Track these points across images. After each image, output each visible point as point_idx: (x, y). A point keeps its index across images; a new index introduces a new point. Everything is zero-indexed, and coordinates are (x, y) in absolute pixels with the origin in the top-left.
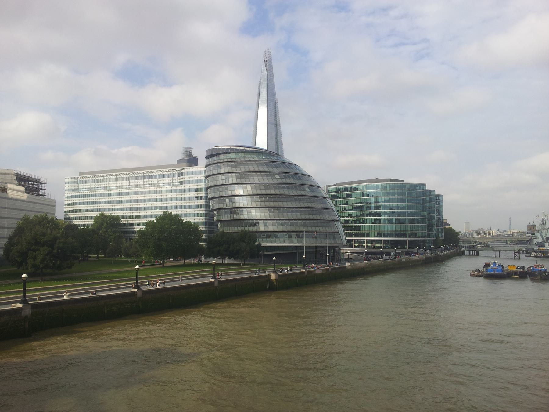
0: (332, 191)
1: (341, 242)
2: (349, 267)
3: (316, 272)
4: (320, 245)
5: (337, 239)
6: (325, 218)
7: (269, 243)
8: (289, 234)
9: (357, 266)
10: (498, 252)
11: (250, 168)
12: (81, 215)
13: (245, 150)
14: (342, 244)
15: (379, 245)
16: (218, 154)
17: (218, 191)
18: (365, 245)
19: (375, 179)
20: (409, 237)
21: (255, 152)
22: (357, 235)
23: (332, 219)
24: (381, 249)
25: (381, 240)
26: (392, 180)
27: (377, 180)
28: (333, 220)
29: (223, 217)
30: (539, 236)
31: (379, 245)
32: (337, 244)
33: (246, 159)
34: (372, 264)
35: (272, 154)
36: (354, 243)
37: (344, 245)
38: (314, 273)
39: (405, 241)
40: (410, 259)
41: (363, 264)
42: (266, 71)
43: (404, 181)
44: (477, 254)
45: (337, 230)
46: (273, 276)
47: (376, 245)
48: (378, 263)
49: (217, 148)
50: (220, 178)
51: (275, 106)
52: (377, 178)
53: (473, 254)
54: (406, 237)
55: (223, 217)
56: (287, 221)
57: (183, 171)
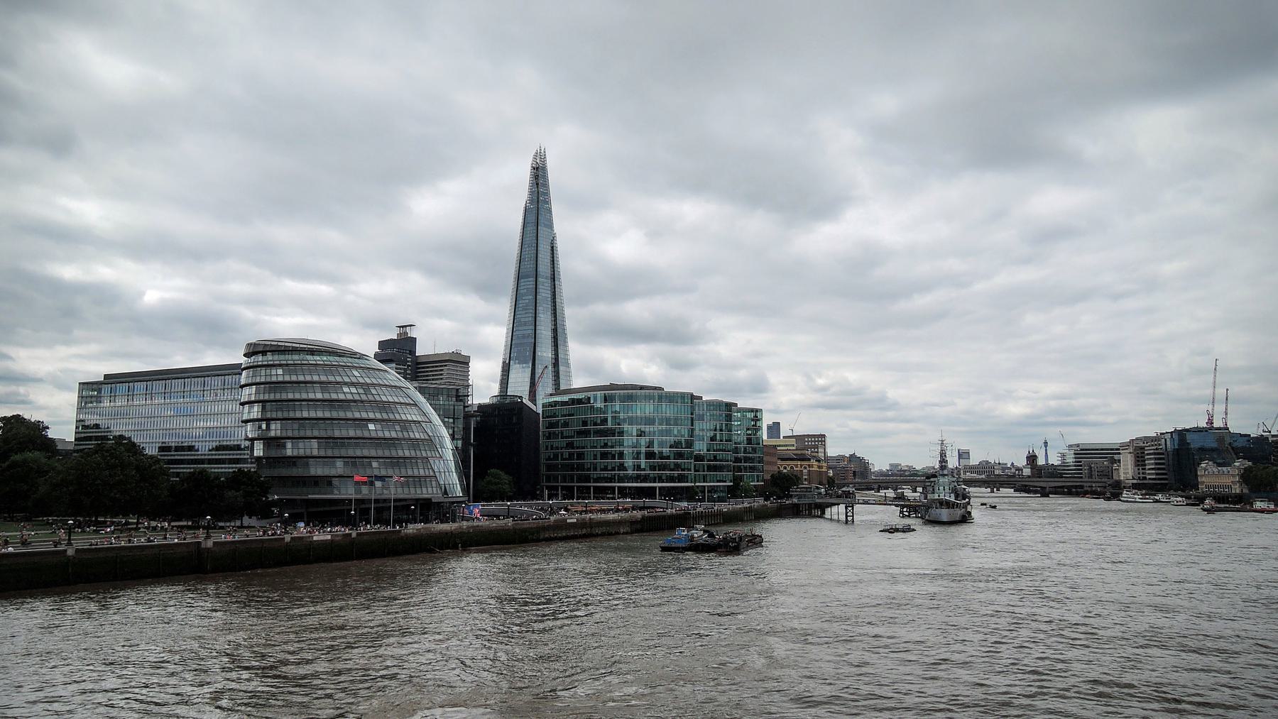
4: (379, 497)
7: (310, 494)
15: (611, 496)
31: (611, 496)
34: (478, 526)
38: (311, 540)
39: (654, 488)
42: (536, 186)
45: (432, 474)
51: (552, 247)
54: (655, 482)
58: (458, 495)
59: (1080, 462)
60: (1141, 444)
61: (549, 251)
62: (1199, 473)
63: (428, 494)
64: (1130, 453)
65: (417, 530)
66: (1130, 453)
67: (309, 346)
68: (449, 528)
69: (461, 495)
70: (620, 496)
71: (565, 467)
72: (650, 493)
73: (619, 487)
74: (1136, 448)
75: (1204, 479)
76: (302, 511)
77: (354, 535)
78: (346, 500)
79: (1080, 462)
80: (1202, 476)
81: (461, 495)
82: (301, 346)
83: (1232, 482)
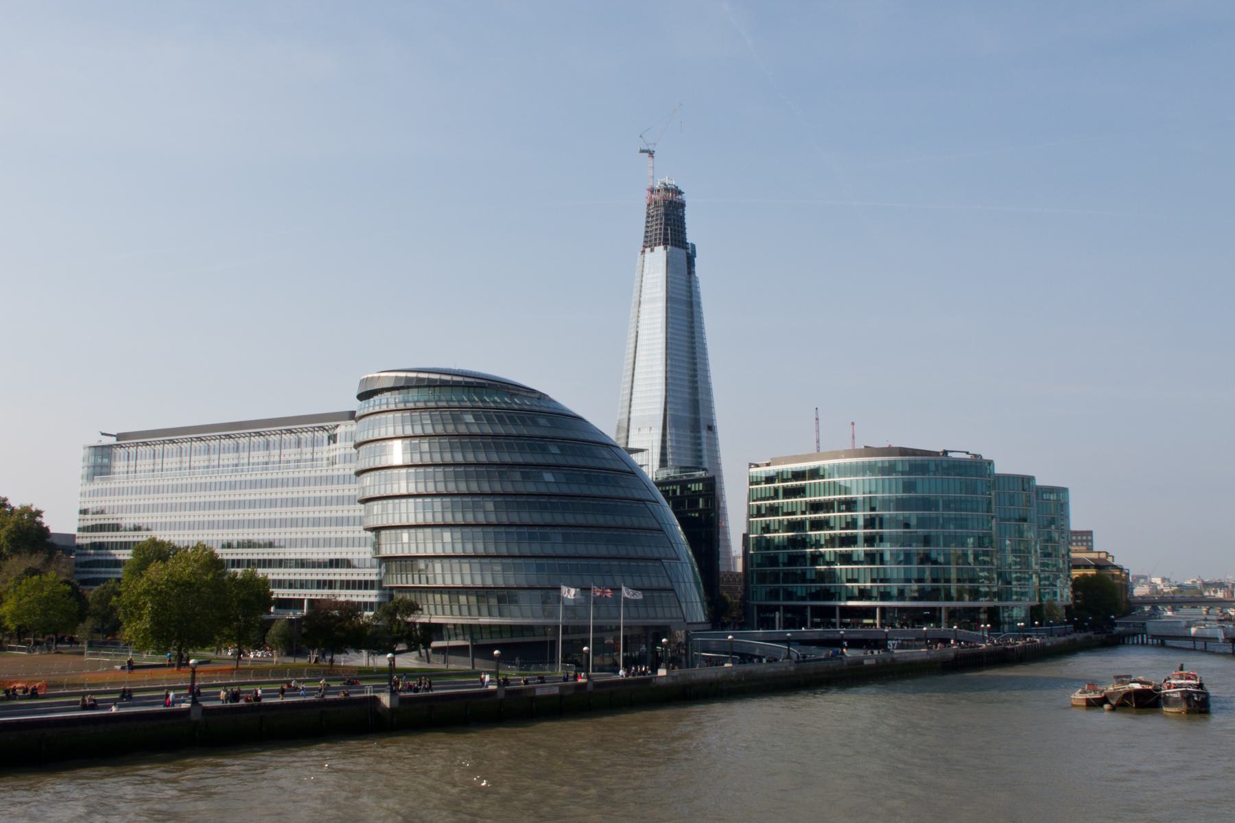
0: (759, 480)
1: (680, 615)
2: (664, 681)
3: (539, 692)
6: (632, 553)
9: (693, 677)
12: (112, 537)
13: (441, 380)
14: (683, 620)
15: (870, 621)
18: (837, 620)
21: (467, 386)
22: (815, 596)
23: (657, 555)
24: (789, 635)
25: (940, 608)
28: (658, 559)
29: (403, 549)
31: (870, 621)
32: (667, 621)
34: (750, 672)
35: (512, 389)
36: (812, 616)
37: (688, 624)
40: (893, 660)
41: (716, 673)
45: (668, 585)
46: (386, 699)
47: (866, 621)
48: (772, 670)
52: (865, 447)
55: (403, 549)
56: (551, 561)
58: (699, 620)
63: (664, 618)
65: (673, 677)
68: (713, 675)
69: (703, 620)
70: (884, 621)
71: (790, 577)
72: (933, 616)
73: (883, 609)
76: (468, 643)
77: (590, 687)
81: (703, 620)
82: (456, 378)
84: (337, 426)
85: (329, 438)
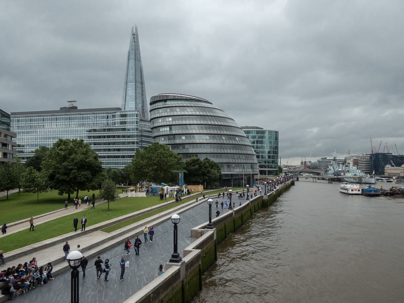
5: (255, 169)
8: (228, 164)
10: (315, 179)
11: (196, 112)
16: (165, 101)
17: (187, 129)
19: (245, 126)
20: (268, 168)
26: (257, 128)
27: (253, 128)
30: (332, 168)
33: (199, 105)
39: (266, 171)
43: (263, 129)
44: (298, 180)
49: (161, 95)
50: (160, 120)
53: (295, 180)
54: (266, 168)
56: (217, 155)
57: (115, 114)
59: (327, 164)
60: (355, 158)
61: (140, 72)
62: (385, 169)
64: (351, 161)
66: (351, 161)
67: (193, 97)
74: (354, 160)
75: (387, 171)
78: (239, 174)
79: (327, 164)
80: (386, 170)
83: (400, 172)
84: (116, 112)
85: (113, 116)
